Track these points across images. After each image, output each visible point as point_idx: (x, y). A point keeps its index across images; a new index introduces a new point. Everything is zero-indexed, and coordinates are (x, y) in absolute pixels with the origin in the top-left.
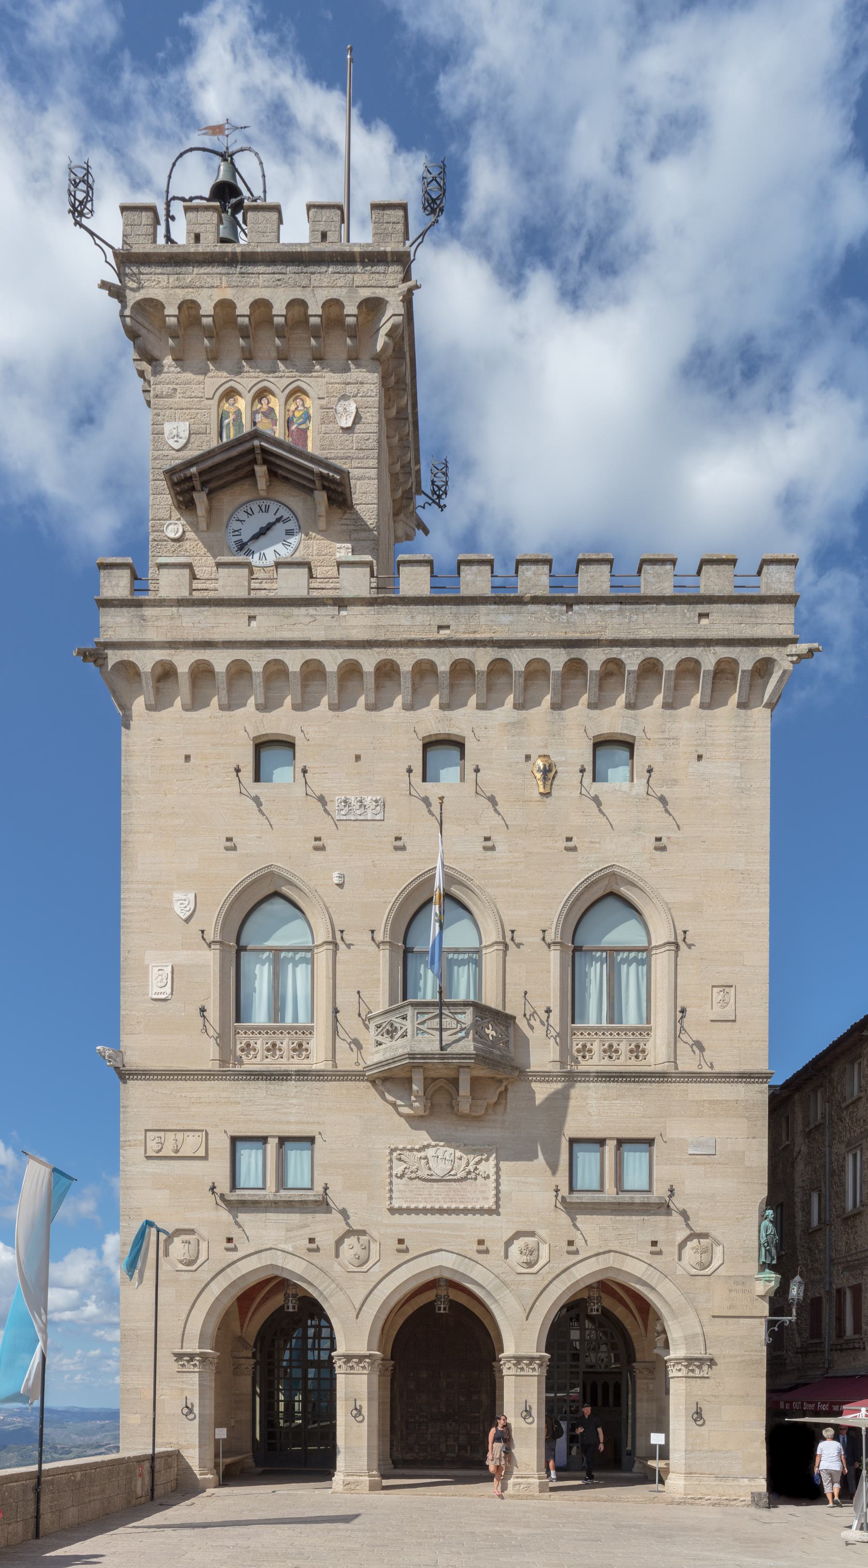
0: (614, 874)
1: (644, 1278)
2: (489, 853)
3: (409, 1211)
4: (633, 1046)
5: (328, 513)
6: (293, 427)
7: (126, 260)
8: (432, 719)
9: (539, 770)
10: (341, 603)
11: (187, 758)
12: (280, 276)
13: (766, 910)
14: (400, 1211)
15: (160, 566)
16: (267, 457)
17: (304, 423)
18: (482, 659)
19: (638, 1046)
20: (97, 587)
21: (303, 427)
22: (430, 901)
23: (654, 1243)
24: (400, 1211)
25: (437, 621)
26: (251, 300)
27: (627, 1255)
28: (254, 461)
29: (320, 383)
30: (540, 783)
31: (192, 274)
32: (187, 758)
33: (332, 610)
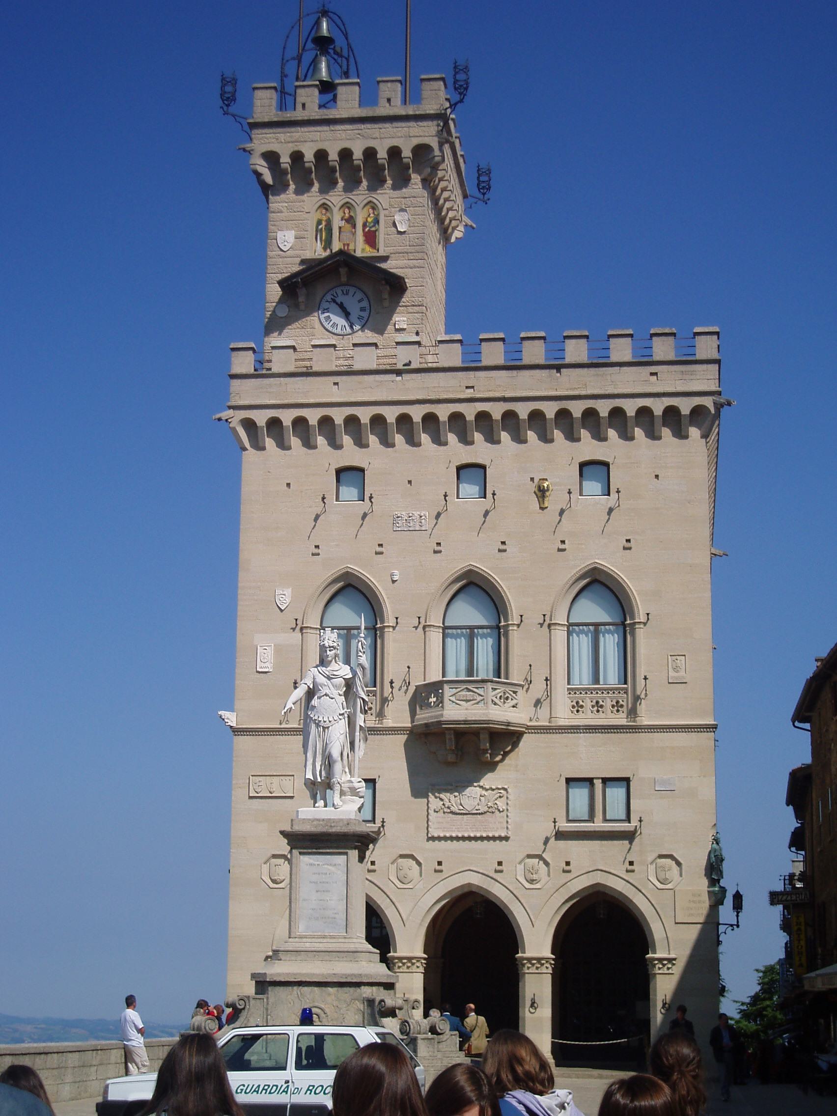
2: (504, 554)
3: (439, 839)
6: (367, 229)
8: (464, 454)
11: (288, 485)
13: (708, 594)
14: (433, 839)
15: (273, 348)
17: (374, 226)
20: (229, 363)
21: (373, 229)
24: (433, 839)
26: (339, 149)
29: (386, 196)
32: (288, 485)
33: (393, 377)
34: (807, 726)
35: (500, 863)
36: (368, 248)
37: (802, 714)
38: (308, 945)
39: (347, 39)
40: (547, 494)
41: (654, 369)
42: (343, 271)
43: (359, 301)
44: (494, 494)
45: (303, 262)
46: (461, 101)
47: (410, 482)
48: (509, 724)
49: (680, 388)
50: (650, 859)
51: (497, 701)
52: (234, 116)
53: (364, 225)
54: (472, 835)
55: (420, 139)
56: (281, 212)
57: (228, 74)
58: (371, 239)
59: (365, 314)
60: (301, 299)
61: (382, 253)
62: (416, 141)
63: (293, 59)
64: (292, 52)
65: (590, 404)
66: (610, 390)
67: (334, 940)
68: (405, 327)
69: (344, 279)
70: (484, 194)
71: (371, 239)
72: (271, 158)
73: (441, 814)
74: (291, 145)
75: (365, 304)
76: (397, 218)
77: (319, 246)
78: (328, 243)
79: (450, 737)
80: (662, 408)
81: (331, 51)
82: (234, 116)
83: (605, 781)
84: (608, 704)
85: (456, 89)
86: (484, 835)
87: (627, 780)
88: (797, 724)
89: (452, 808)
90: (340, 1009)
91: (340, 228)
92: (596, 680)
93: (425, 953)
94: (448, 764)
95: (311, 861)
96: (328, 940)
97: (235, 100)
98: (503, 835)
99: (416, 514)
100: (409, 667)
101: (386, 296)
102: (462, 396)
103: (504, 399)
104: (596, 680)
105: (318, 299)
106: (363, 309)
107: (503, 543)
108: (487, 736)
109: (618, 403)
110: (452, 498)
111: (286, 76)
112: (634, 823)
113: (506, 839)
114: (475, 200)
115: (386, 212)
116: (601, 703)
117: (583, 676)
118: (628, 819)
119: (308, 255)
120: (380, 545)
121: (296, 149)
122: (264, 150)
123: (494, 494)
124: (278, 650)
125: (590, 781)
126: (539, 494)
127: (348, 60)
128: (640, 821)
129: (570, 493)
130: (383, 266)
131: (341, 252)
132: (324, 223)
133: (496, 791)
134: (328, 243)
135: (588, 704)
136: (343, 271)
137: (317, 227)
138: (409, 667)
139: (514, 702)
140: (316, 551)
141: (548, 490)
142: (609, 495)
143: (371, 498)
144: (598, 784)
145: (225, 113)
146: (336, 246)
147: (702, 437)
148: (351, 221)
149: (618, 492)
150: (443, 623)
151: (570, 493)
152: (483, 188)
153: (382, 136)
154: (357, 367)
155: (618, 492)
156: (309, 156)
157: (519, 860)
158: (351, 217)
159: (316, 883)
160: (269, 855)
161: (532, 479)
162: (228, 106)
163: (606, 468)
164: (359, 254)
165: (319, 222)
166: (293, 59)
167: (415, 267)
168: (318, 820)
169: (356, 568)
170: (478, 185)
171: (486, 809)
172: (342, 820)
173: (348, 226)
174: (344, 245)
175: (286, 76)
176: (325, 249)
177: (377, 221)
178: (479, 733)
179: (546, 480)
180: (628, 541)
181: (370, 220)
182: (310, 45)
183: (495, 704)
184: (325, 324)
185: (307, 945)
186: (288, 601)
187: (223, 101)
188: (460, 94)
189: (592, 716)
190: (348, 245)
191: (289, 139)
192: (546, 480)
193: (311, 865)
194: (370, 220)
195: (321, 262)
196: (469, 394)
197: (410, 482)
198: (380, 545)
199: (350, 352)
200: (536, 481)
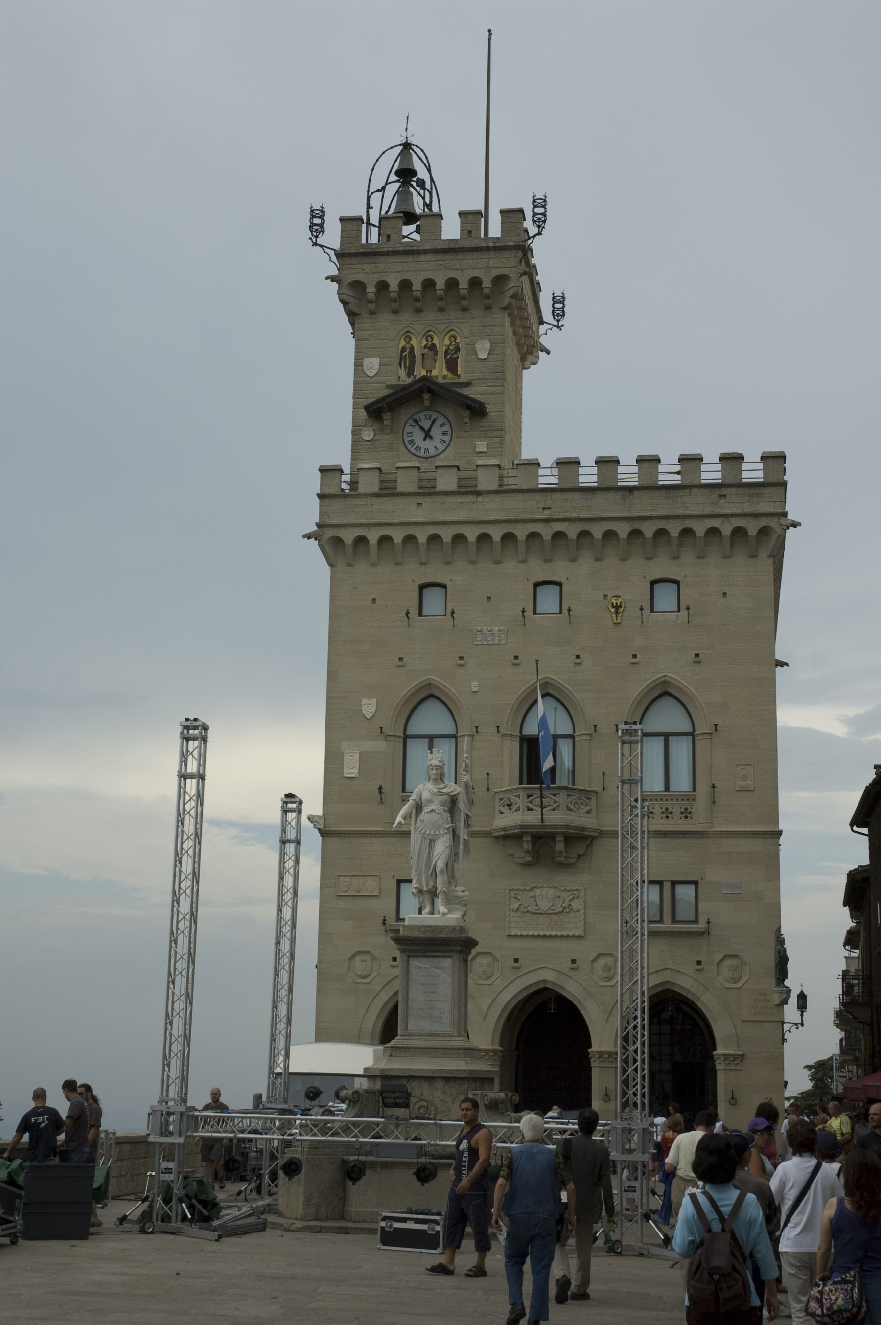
0: (666, 682)
1: (692, 990)
2: (579, 667)
4: (683, 810)
5: (471, 419)
7: (340, 255)
9: (613, 607)
10: (479, 494)
12: (442, 263)
16: (430, 390)
18: (572, 531)
19: (686, 809)
21: (455, 356)
22: (536, 702)
23: (699, 963)
25: (543, 504)
26: (422, 279)
27: (679, 971)
28: (422, 391)
30: (614, 616)
31: (383, 263)
32: (374, 600)
34: (865, 830)
35: (574, 961)
36: (450, 375)
37: (860, 819)
38: (416, 1042)
39: (429, 170)
40: (621, 610)
41: (724, 491)
42: (426, 396)
43: (442, 426)
44: (569, 610)
45: (389, 387)
46: (540, 234)
47: (489, 598)
48: (583, 829)
49: (748, 510)
50: (718, 957)
51: (571, 807)
52: (321, 246)
53: (446, 353)
54: (548, 934)
55: (500, 270)
56: (367, 339)
57: (317, 207)
58: (452, 365)
59: (447, 438)
60: (386, 423)
61: (462, 380)
62: (496, 272)
63: (378, 191)
64: (377, 184)
65: (661, 524)
66: (681, 511)
67: (440, 1038)
68: (485, 450)
69: (427, 403)
70: (558, 321)
71: (452, 365)
72: (358, 286)
73: (518, 914)
74: (376, 275)
75: (447, 428)
76: (478, 345)
77: (402, 372)
78: (410, 372)
79: (527, 838)
80: (730, 529)
81: (414, 184)
82: (321, 246)
83: (674, 883)
84: (677, 810)
85: (534, 221)
86: (559, 934)
87: (695, 883)
88: (855, 828)
89: (529, 909)
90: (446, 1102)
91: (423, 355)
92: (667, 789)
93: (500, 1046)
94: (526, 865)
95: (420, 965)
96: (435, 1038)
97: (323, 232)
98: (577, 934)
99: (496, 629)
100: (488, 774)
101: (467, 420)
102: (539, 517)
103: (580, 520)
104: (667, 789)
105: (402, 424)
106: (444, 433)
107: (578, 657)
108: (562, 839)
109: (688, 524)
110: (529, 613)
111: (371, 208)
112: (702, 925)
113: (579, 937)
114: (550, 327)
115: (467, 340)
116: (670, 810)
117: (654, 783)
118: (696, 921)
119: (393, 381)
120: (461, 658)
121: (382, 279)
122: (351, 280)
123: (569, 610)
124: (363, 756)
125: (660, 883)
126: (613, 610)
127: (431, 194)
128: (708, 922)
129: (642, 609)
130: (465, 391)
131: (424, 378)
132: (408, 351)
133: (570, 893)
134: (410, 372)
135: (657, 810)
136: (426, 396)
137: (401, 354)
138: (488, 774)
139: (588, 808)
140: (400, 663)
141: (621, 607)
142: (679, 611)
143: (453, 613)
144: (667, 887)
145: (315, 244)
146: (420, 372)
147: (769, 556)
148: (432, 348)
149: (688, 609)
150: (521, 732)
151: (642, 609)
152: (558, 315)
153: (464, 267)
154: (440, 487)
155: (688, 609)
156: (394, 285)
157: (591, 958)
158: (434, 345)
159: (423, 984)
160: (354, 952)
161: (606, 596)
162: (316, 237)
163: (676, 586)
164: (440, 380)
165: (404, 349)
166: (378, 191)
167: (494, 393)
168: (426, 926)
169: (437, 679)
170: (553, 312)
171: (560, 909)
172: (448, 926)
173: (430, 353)
174: (427, 371)
175: (371, 208)
176: (409, 375)
177: (457, 349)
178: (554, 837)
179: (619, 597)
180: (697, 655)
181: (451, 348)
182: (393, 177)
183: (570, 810)
184: (409, 447)
185: (416, 1042)
186: (374, 709)
187: (312, 232)
188: (539, 226)
189: (664, 821)
190: (431, 371)
191: (375, 270)
192: (619, 597)
193: (419, 968)
194: (451, 348)
195: (405, 388)
196: (547, 514)
197: (489, 598)
198: (461, 658)
199: (433, 474)
200: (610, 596)
